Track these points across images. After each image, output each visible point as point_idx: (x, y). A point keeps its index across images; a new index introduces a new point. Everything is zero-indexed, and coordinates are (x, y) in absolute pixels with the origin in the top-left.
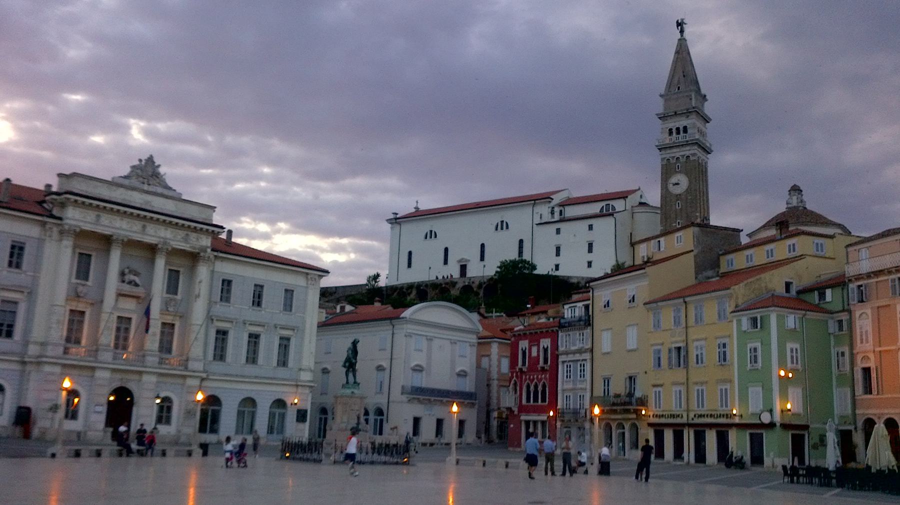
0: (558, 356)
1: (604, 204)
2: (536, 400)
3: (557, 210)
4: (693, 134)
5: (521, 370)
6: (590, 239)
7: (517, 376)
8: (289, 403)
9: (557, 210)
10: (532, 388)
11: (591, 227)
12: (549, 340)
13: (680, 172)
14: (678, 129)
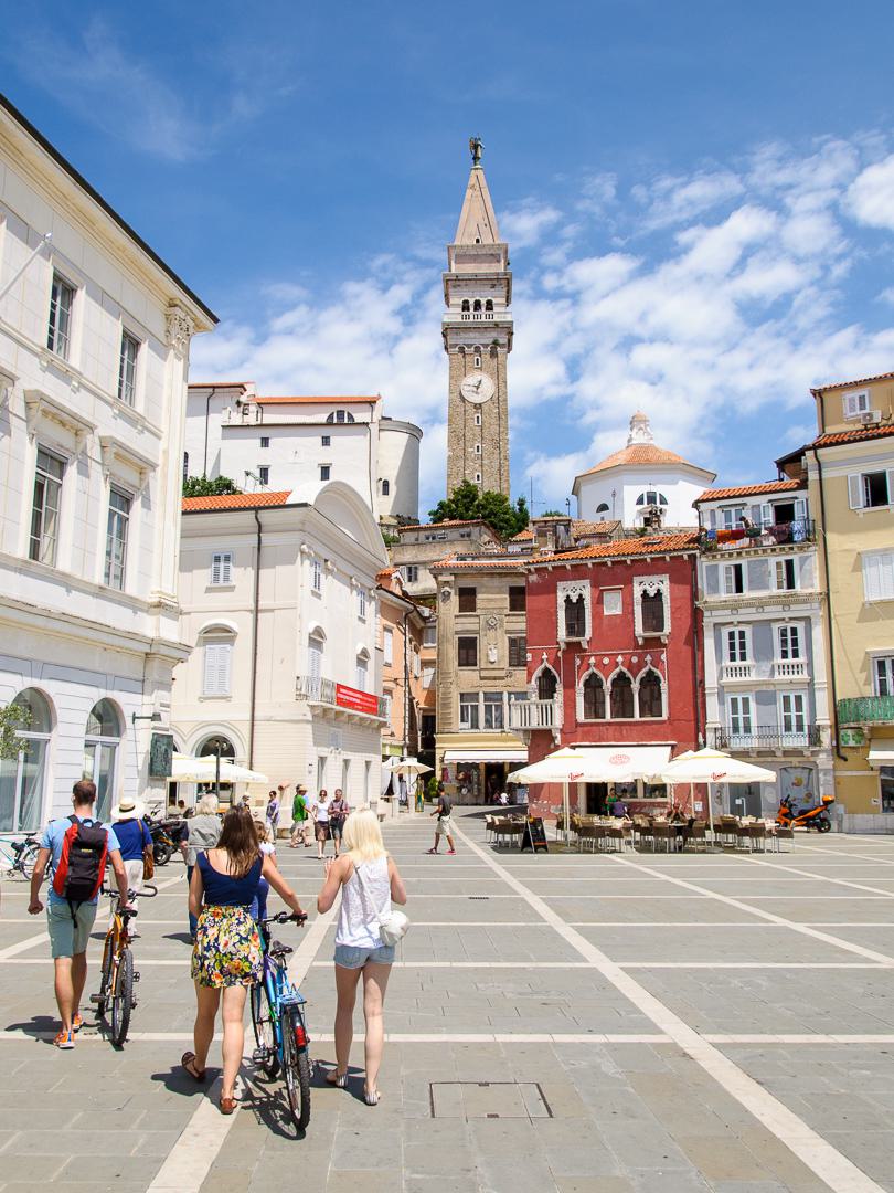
0: (697, 615)
1: (334, 409)
2: (623, 707)
3: (253, 408)
4: (499, 315)
5: (573, 648)
6: (325, 461)
7: (556, 663)
8: (127, 713)
9: (253, 408)
10: (607, 686)
11: (326, 441)
12: (666, 578)
13: (481, 369)
14: (477, 305)
